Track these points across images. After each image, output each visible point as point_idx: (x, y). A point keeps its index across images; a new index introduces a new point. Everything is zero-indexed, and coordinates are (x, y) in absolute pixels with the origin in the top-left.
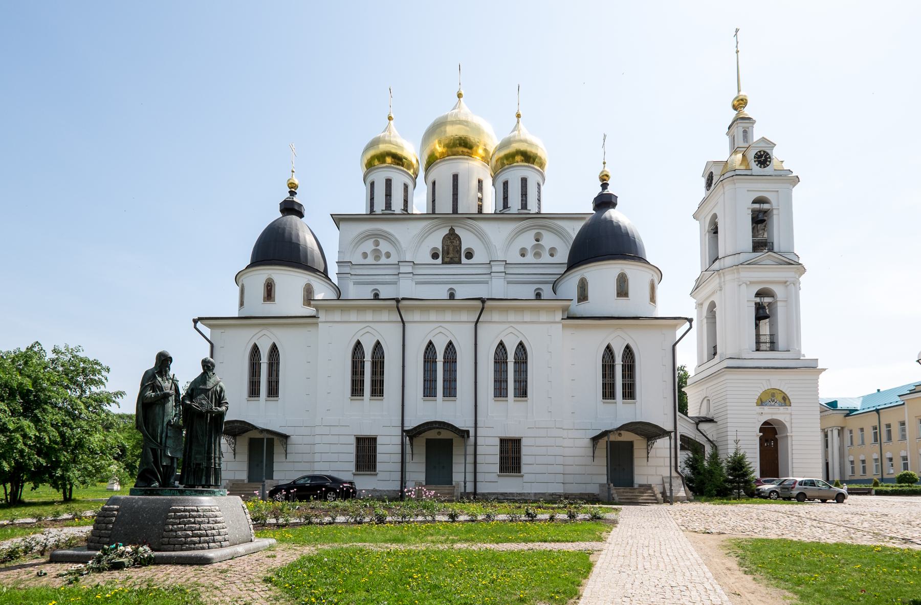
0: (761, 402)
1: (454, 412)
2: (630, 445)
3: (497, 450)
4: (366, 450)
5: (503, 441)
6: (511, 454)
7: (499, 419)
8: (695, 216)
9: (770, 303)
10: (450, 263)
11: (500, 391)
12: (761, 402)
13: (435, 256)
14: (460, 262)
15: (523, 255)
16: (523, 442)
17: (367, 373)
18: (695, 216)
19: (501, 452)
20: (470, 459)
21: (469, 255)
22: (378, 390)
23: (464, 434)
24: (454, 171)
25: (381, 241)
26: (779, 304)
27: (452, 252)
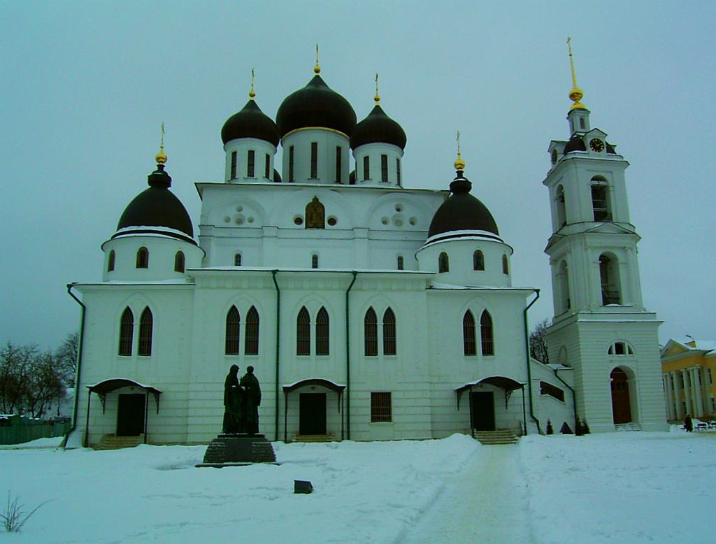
1: (326, 368)
2: (490, 395)
3: (369, 403)
5: (373, 394)
6: (381, 406)
7: (371, 374)
11: (371, 350)
14: (323, 227)
15: (385, 222)
16: (393, 396)
24: (314, 140)
25: (244, 208)
26: (620, 266)
27: (315, 217)
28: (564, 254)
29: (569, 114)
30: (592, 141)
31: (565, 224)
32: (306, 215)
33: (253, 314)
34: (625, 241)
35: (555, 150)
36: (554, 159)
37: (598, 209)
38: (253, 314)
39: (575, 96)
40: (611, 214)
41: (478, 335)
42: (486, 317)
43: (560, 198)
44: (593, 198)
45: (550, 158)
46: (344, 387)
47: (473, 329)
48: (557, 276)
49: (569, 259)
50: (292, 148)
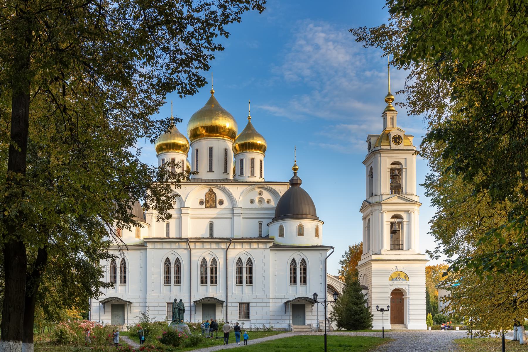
0: (392, 279)
4: (176, 310)
5: (240, 304)
6: (244, 310)
8: (364, 163)
10: (210, 207)
11: (239, 281)
12: (392, 279)
13: (201, 203)
14: (215, 207)
16: (251, 305)
17: (172, 273)
18: (364, 163)
19: (240, 309)
20: (225, 313)
21: (221, 202)
22: (178, 281)
23: (221, 303)
31: (372, 195)
32: (206, 199)
33: (178, 261)
36: (369, 149)
37: (394, 184)
38: (178, 261)
41: (298, 273)
42: (303, 261)
45: (367, 147)
46: (224, 301)
47: (295, 269)
50: (197, 151)
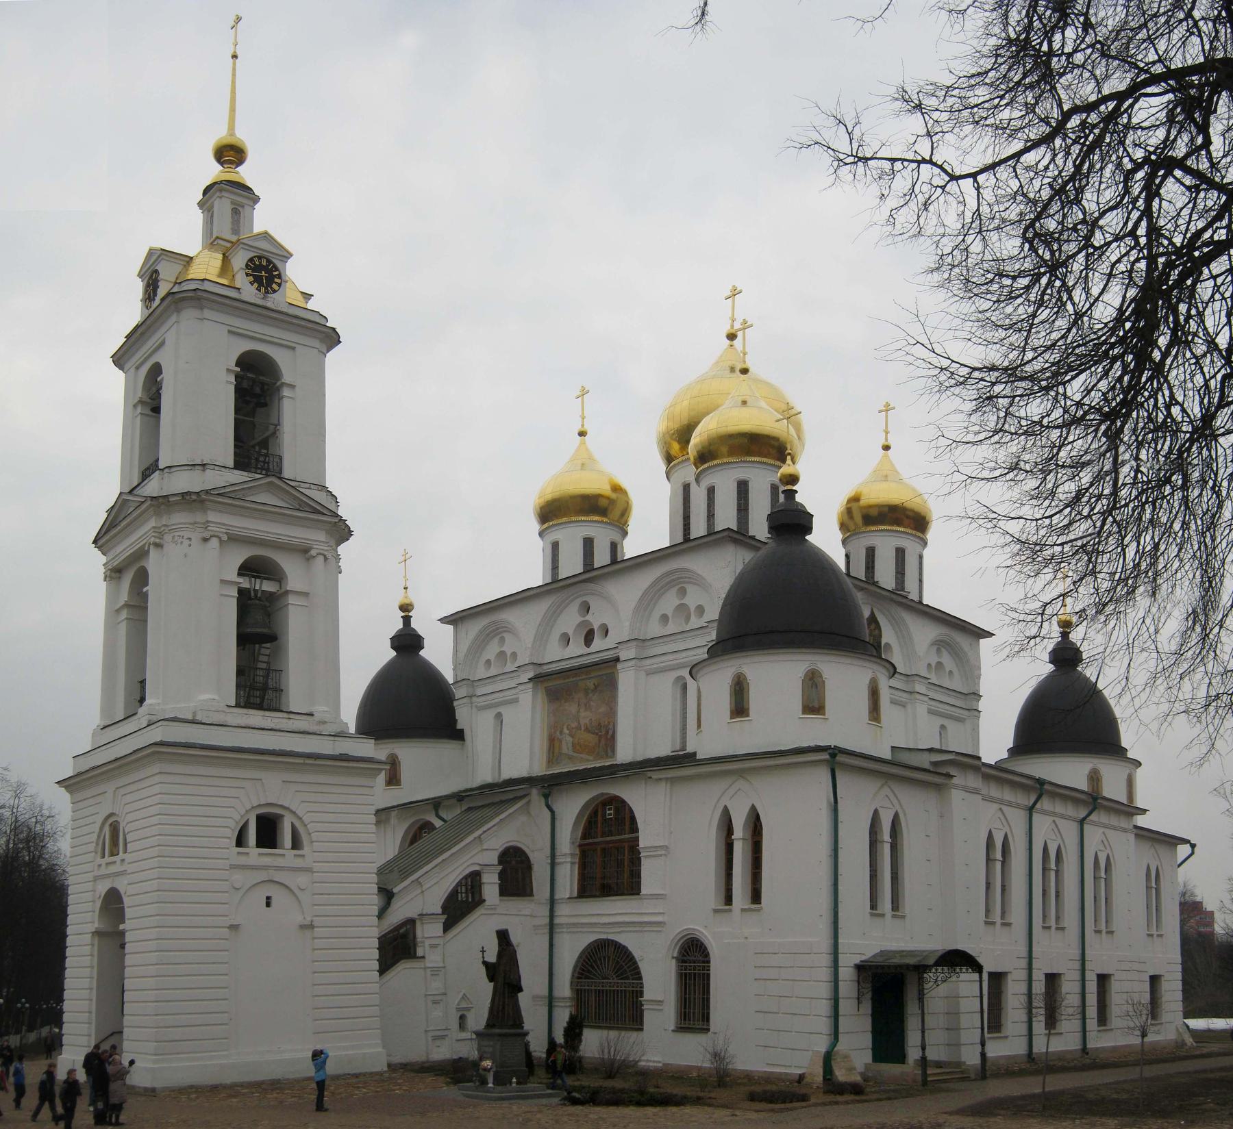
9: (271, 594)
26: (292, 600)
28: (142, 554)
29: (205, 192)
30: (251, 260)
34: (317, 537)
35: (156, 271)
39: (230, 154)
40: (281, 458)
43: (149, 402)
44: (236, 413)
48: (118, 611)
49: (153, 563)
